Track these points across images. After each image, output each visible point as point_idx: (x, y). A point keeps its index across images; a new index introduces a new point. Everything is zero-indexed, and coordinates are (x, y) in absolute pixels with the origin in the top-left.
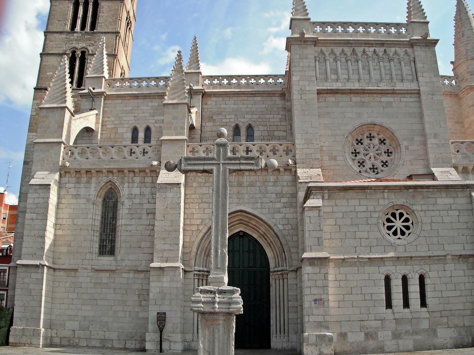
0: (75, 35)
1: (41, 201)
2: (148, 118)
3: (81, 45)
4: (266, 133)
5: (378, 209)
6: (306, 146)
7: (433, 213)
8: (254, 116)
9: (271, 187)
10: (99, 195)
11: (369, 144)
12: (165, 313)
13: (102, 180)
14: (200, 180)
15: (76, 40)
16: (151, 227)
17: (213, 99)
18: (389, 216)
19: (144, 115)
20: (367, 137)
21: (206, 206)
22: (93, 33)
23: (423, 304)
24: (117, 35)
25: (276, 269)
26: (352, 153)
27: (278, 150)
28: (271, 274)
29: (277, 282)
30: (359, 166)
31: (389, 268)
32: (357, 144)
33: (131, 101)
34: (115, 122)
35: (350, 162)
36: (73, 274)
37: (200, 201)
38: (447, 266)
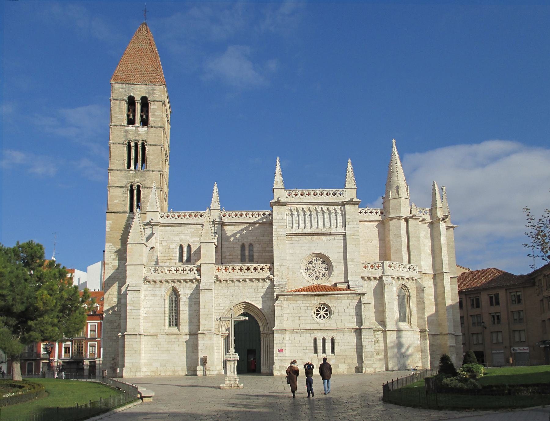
0: (131, 172)
3: (136, 180)
4: (260, 249)
5: (311, 305)
6: (279, 267)
7: (340, 308)
8: (254, 238)
9: (261, 290)
11: (316, 264)
14: (223, 286)
16: (197, 311)
17: (228, 227)
18: (318, 309)
19: (185, 237)
20: (315, 260)
21: (226, 299)
22: (144, 171)
23: (333, 351)
24: (161, 172)
25: (264, 332)
26: (306, 269)
28: (261, 335)
29: (264, 339)
30: (309, 277)
31: (316, 334)
32: (309, 264)
33: (177, 227)
34: (168, 242)
35: (304, 275)
37: (223, 297)
38: (345, 334)
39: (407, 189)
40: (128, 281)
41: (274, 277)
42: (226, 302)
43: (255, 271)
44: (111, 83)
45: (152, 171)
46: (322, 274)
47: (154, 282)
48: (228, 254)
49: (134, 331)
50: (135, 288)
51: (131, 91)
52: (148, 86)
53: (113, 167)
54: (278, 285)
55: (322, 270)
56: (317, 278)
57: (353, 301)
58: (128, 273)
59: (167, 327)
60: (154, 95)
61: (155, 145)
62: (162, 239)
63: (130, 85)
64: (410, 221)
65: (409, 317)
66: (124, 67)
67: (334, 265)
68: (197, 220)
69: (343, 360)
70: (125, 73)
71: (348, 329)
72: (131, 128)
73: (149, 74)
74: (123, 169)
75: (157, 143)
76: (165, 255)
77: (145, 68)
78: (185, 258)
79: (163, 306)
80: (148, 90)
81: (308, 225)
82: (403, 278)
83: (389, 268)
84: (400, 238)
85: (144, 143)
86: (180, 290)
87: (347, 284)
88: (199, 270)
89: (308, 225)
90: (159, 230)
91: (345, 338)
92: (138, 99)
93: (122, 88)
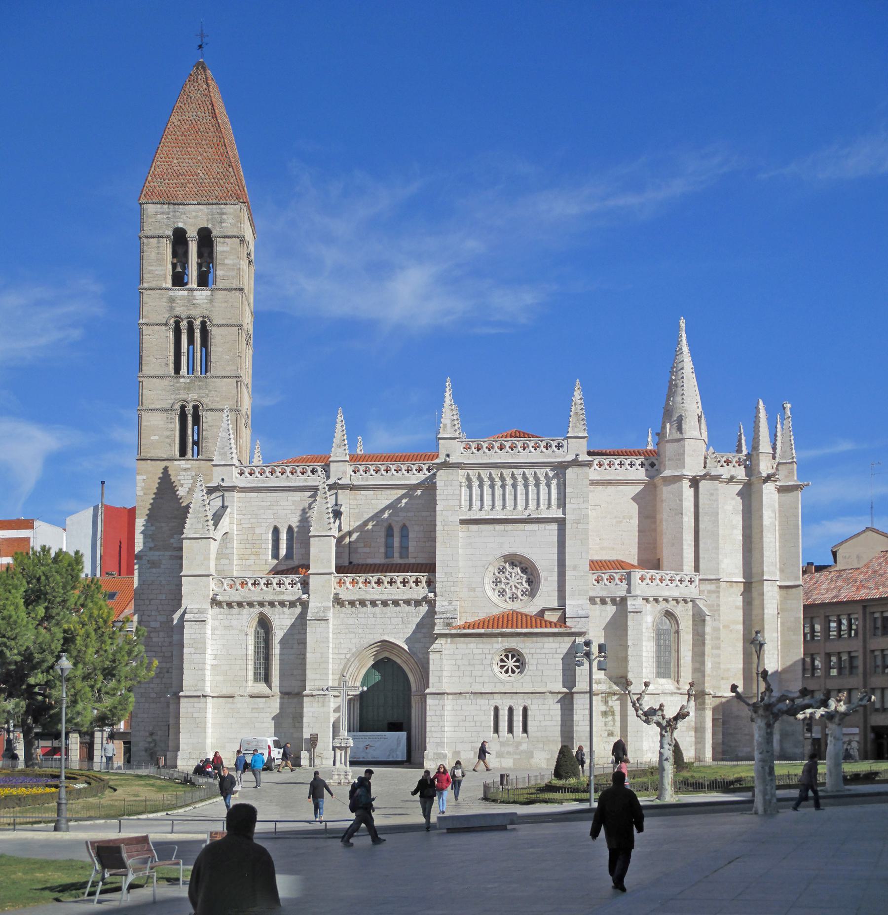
0: (182, 380)
1: (198, 636)
2: (289, 516)
3: (192, 397)
6: (446, 579)
7: (539, 656)
8: (409, 514)
10: (251, 625)
11: (511, 573)
12: (317, 735)
13: (253, 612)
14: (347, 611)
15: (185, 388)
16: (302, 657)
19: (284, 512)
21: (352, 635)
22: (206, 377)
23: (525, 730)
24: (238, 379)
26: (493, 582)
27: (420, 582)
30: (499, 596)
32: (499, 573)
34: (252, 521)
35: (489, 593)
36: (230, 700)
37: (347, 631)
39: (699, 421)
40: (185, 603)
41: (435, 596)
42: (353, 641)
43: (404, 586)
44: (141, 204)
45: (222, 377)
46: (522, 591)
47: (230, 605)
48: (362, 545)
49: (196, 691)
50: (198, 617)
51: (179, 218)
52: (210, 207)
53: (147, 370)
54: (441, 613)
55: (522, 583)
56: (514, 598)
57: (563, 645)
58: (185, 589)
59: (250, 683)
60: (223, 225)
61: (227, 325)
62: (242, 517)
63: (176, 207)
64: (703, 485)
65: (676, 669)
66: (164, 167)
67: (543, 575)
68: (305, 480)
69: (541, 745)
70: (167, 181)
71: (551, 693)
72: (181, 293)
73: (213, 180)
74: (166, 374)
75: (230, 322)
76: (248, 546)
77: (205, 168)
78: (283, 551)
79: (244, 646)
80: (212, 215)
81: (499, 504)
82: (666, 600)
83: (640, 581)
84: (680, 515)
85: (206, 322)
86: (274, 619)
87: (562, 611)
88: (305, 585)
89: (499, 504)
90: (235, 500)
91: (547, 707)
92: (192, 233)
93: (163, 213)
